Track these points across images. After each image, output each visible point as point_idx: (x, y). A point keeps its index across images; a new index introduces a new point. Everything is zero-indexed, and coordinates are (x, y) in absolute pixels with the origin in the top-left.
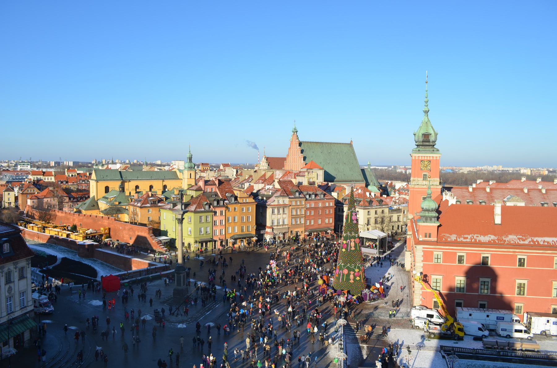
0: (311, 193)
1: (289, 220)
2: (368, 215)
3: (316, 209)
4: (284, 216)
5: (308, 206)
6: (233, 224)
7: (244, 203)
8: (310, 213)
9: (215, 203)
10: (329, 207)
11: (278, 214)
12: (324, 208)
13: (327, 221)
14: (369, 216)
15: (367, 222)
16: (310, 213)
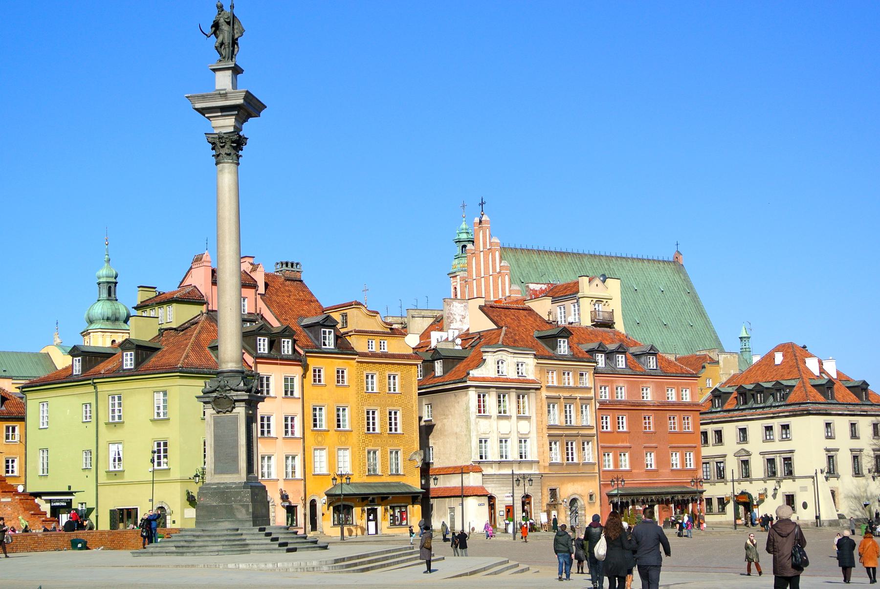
0: (612, 347)
1: (540, 446)
2: (828, 437)
3: (635, 407)
4: (524, 427)
5: (605, 395)
6: (332, 437)
7: (374, 355)
8: (617, 423)
9: (263, 346)
10: (680, 408)
11: (499, 418)
12: (664, 408)
13: (676, 460)
14: (830, 444)
15: (824, 465)
16: (617, 423)
